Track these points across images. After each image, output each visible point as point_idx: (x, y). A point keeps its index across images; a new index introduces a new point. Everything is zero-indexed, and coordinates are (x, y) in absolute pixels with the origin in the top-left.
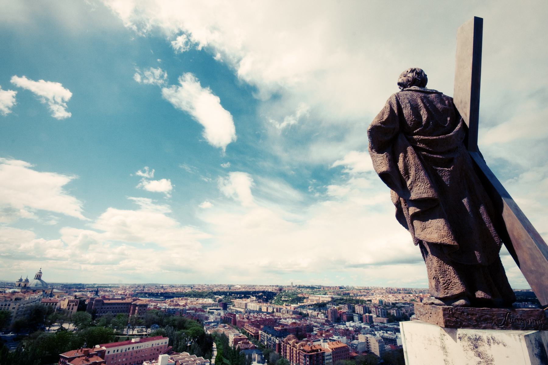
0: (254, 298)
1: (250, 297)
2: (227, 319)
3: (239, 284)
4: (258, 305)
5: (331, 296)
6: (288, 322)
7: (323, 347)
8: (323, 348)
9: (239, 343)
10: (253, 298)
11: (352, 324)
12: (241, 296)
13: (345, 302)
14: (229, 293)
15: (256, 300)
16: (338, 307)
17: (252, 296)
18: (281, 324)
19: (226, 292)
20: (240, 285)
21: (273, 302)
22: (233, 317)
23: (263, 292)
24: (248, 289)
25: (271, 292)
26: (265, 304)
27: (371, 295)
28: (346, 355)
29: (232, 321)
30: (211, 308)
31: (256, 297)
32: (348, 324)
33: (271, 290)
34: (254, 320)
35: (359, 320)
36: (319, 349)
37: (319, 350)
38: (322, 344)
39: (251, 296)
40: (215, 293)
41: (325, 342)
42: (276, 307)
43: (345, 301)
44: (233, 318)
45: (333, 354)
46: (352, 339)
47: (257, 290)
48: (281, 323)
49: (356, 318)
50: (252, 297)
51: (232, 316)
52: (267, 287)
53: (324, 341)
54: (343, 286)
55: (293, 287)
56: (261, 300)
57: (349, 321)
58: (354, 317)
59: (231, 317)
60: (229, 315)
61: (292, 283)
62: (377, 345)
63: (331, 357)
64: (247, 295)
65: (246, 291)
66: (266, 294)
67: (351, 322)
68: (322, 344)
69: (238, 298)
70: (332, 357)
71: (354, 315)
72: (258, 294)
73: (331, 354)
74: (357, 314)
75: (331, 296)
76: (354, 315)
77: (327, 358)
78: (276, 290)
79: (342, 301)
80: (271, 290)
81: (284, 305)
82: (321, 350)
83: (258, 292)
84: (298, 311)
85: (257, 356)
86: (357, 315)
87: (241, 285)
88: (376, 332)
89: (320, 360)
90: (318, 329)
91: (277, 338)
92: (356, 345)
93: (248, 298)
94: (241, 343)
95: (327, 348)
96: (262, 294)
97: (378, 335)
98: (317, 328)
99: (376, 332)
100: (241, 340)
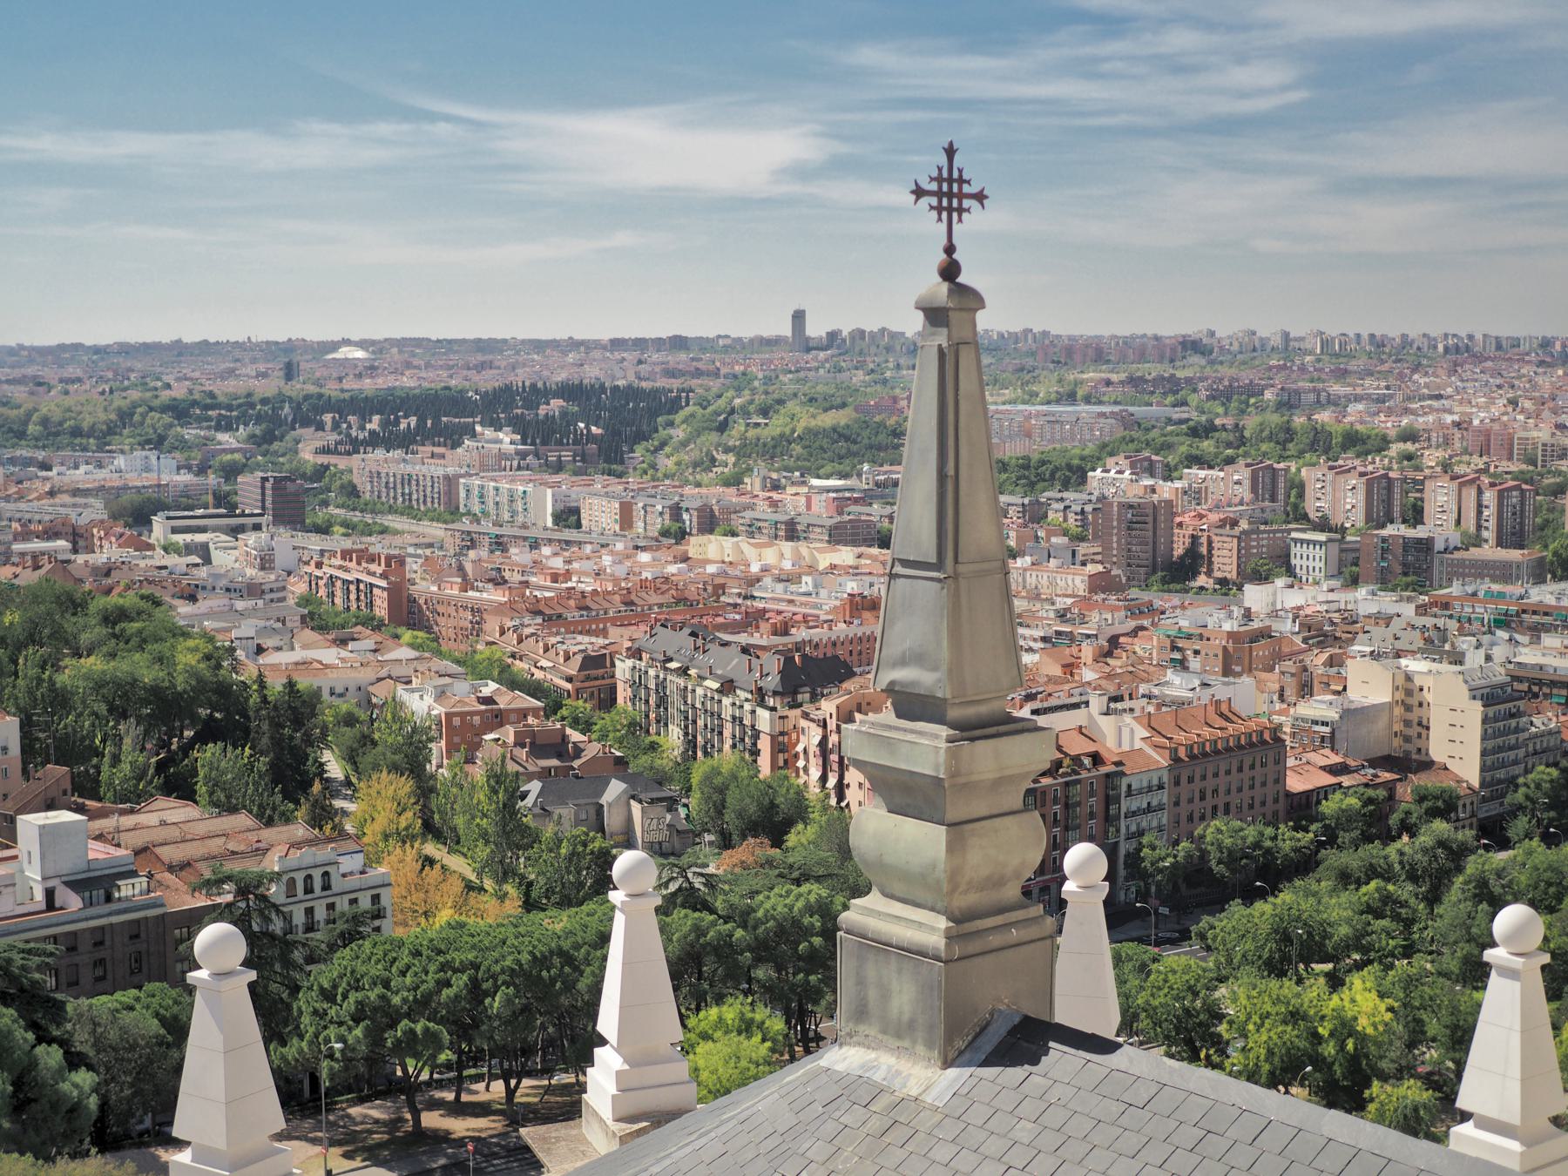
0: (506, 440)
1: (474, 435)
2: (339, 593)
3: (355, 338)
4: (549, 492)
5: (1116, 409)
6: (812, 599)
7: (1111, 742)
8: (1109, 750)
9: (488, 737)
10: (501, 435)
11: (1293, 599)
12: (397, 422)
13: (1229, 452)
14: (297, 408)
15: (523, 455)
16: (1178, 484)
17: (482, 424)
18: (764, 611)
19: (264, 401)
20: (362, 344)
21: (666, 463)
22: (384, 576)
23: (570, 391)
24: (444, 374)
25: (632, 393)
26: (599, 482)
27: (1423, 398)
28: (1202, 798)
29: (378, 602)
30: (172, 514)
31: (519, 425)
32: (1255, 596)
33: (631, 377)
34: (552, 594)
35: (1329, 577)
36: (1088, 755)
37: (1087, 761)
38: (1106, 725)
39: (478, 428)
40: (180, 411)
41: (1116, 712)
42: (698, 504)
43: (1229, 445)
44: (383, 584)
45: (1177, 783)
46: (1287, 693)
47: (521, 378)
48: (760, 605)
49: (1310, 556)
50: (489, 433)
51: (373, 567)
52: (597, 354)
53: (1112, 705)
54: (1212, 334)
55: (808, 350)
56: (567, 456)
57: (1261, 577)
58: (1296, 550)
59: (373, 574)
60: (353, 565)
61: (799, 317)
62: (1475, 712)
63: (1164, 797)
64: (444, 419)
65: (426, 385)
66: (598, 406)
67: (1280, 582)
68: (1106, 725)
69: (374, 441)
70: (1165, 800)
71: (1294, 535)
72: (531, 404)
73: (1165, 779)
74: (1323, 525)
75: (1116, 409)
76: (1294, 535)
77: (1134, 808)
78: (671, 373)
79: (1207, 445)
80: (631, 377)
81: (753, 483)
82: (1097, 759)
83: (536, 394)
84: (870, 524)
85: (643, 811)
86: (1322, 537)
87: (373, 343)
88: (1465, 644)
89: (1092, 815)
90: (1044, 639)
91: (771, 702)
92: (1325, 724)
93: (453, 437)
94: (511, 739)
95: (1138, 744)
96: (564, 414)
97: (1474, 659)
98: (1039, 633)
99: (1465, 644)
100: (498, 719)
